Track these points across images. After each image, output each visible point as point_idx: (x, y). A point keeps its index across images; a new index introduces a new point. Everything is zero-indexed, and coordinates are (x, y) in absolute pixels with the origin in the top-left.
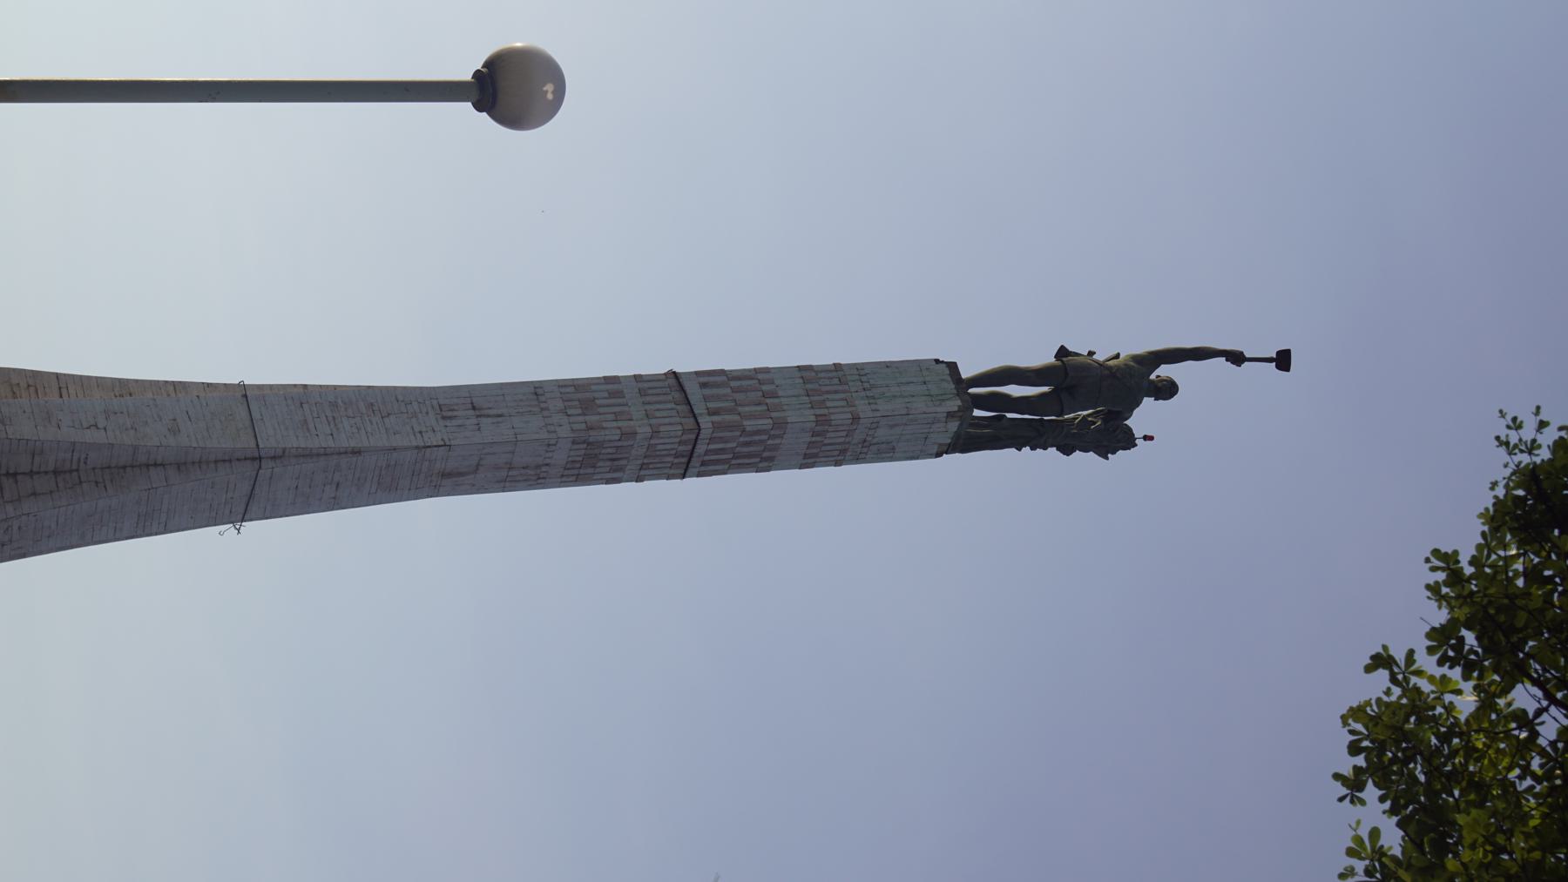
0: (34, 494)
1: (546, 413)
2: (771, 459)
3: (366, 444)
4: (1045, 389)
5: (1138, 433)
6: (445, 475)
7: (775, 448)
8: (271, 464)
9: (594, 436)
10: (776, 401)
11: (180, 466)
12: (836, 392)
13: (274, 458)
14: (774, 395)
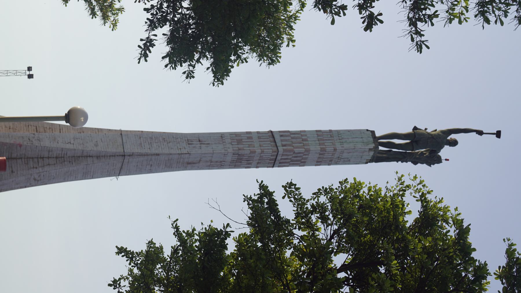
0: (49, 165)
1: (224, 144)
2: (305, 162)
3: (161, 152)
4: (408, 141)
5: (443, 158)
6: (188, 163)
7: (306, 159)
8: (129, 157)
9: (241, 152)
10: (307, 142)
11: (98, 157)
12: (329, 140)
13: (129, 156)
14: (306, 140)
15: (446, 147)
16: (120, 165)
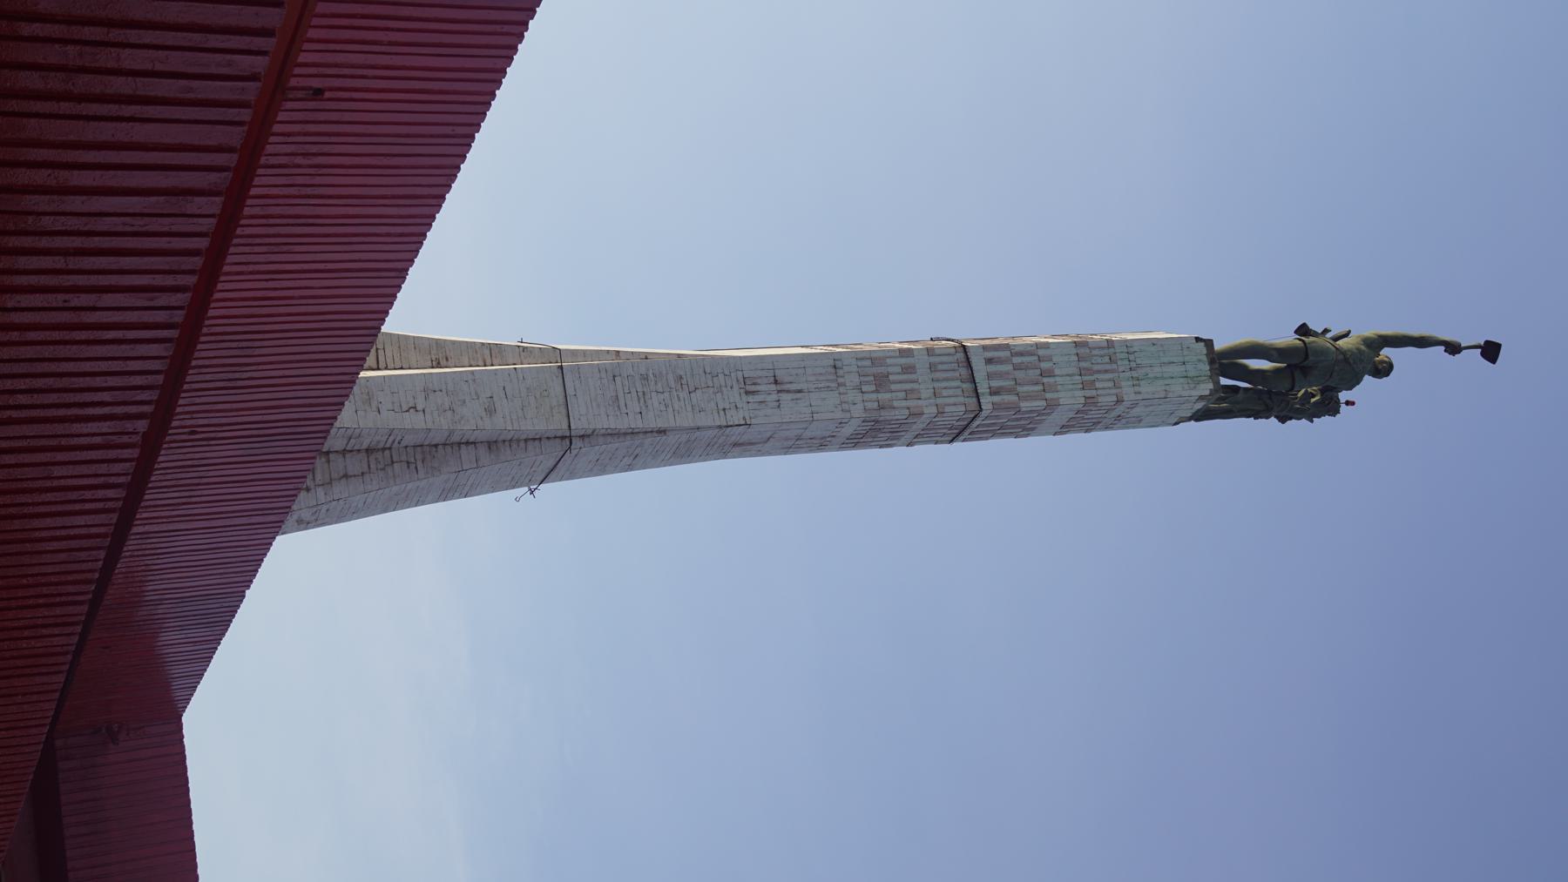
0: (346, 476)
1: (842, 389)
3: (672, 424)
6: (735, 445)
9: (886, 415)
10: (1051, 380)
12: (1106, 371)
13: (582, 437)
14: (1049, 373)
15: (1368, 380)
16: (551, 463)
